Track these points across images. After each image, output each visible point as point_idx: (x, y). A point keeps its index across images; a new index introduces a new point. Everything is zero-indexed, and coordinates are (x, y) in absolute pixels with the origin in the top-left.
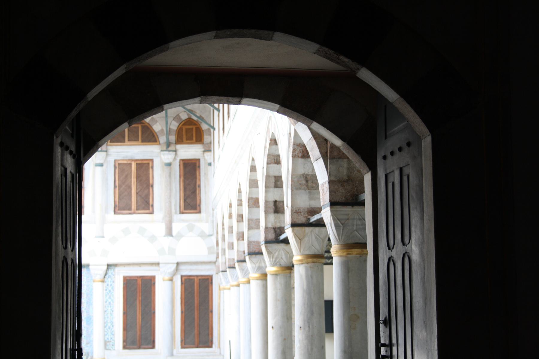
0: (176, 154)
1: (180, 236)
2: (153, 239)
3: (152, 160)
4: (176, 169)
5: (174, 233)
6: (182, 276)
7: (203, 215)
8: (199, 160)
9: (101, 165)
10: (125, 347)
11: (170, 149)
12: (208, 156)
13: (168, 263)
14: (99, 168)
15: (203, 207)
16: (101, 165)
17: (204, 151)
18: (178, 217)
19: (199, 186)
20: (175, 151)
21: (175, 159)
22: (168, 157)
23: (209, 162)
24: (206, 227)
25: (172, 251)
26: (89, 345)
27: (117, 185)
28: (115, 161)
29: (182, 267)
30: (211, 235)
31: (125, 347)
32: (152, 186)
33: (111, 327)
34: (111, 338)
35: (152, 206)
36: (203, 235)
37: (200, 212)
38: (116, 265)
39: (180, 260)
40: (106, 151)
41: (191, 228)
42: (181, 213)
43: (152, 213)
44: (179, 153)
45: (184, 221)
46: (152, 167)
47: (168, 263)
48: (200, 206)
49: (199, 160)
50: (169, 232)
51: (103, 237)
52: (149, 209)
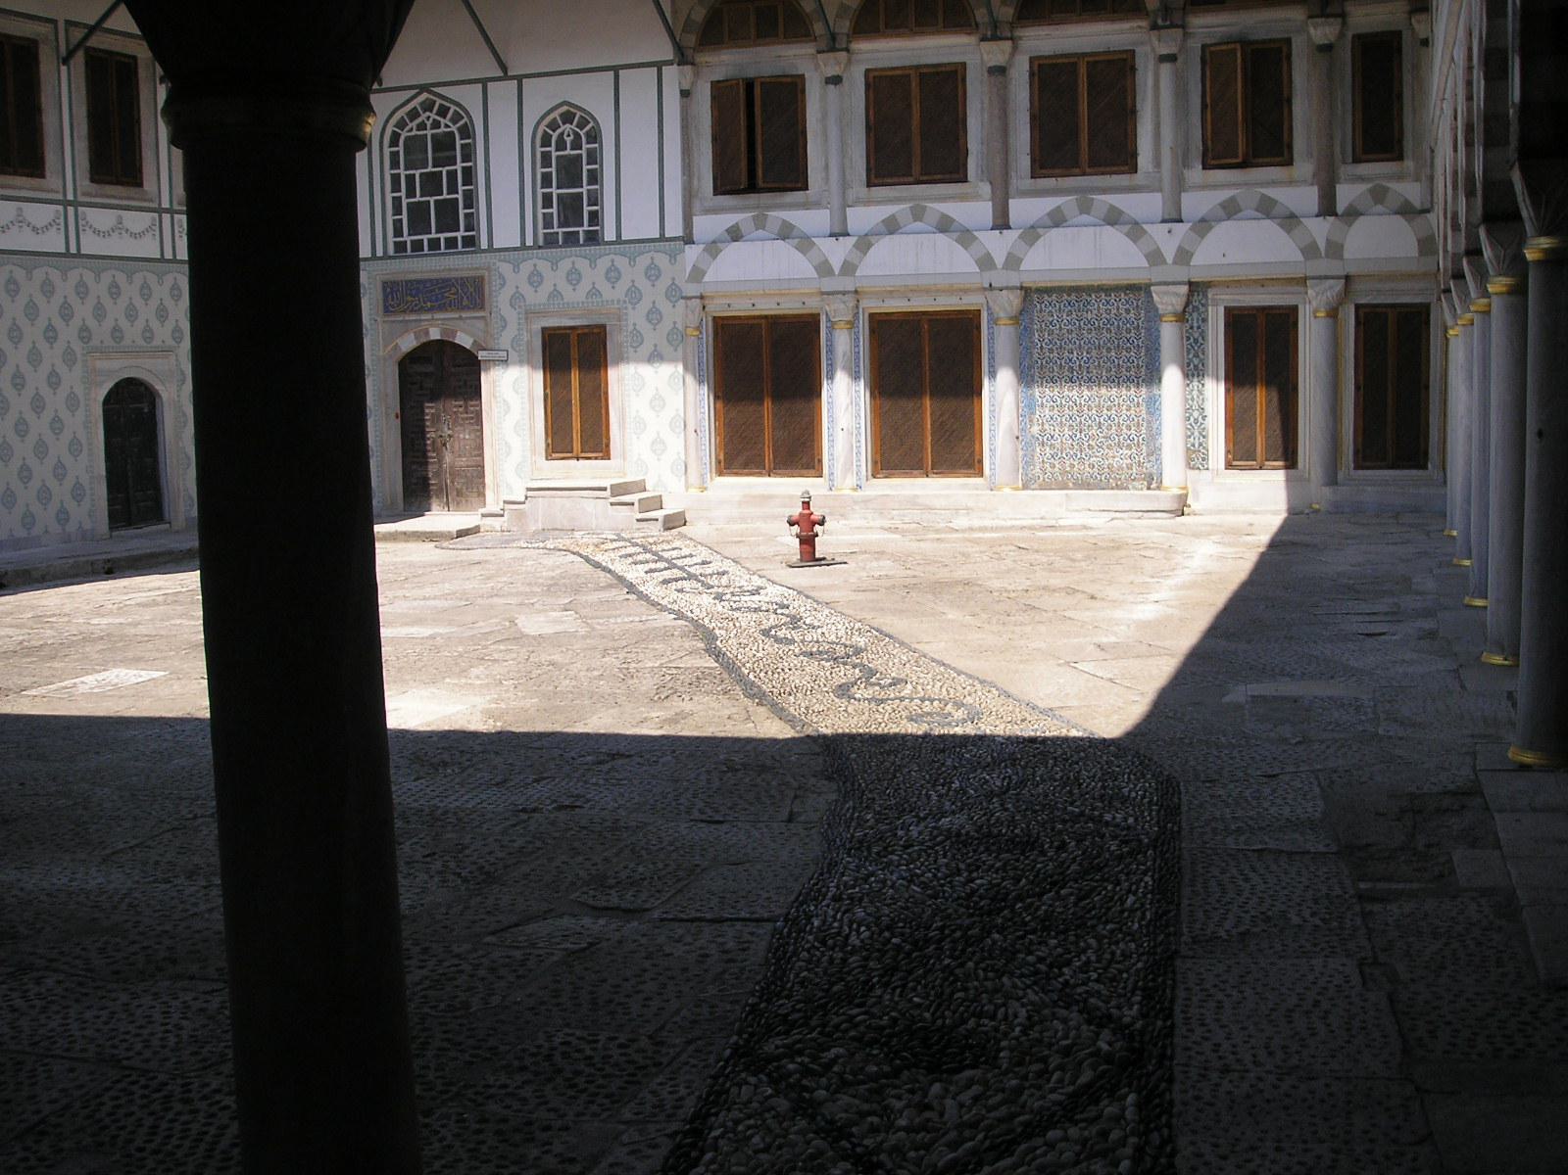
0: (1344, 24)
1: (1353, 214)
2: (1290, 221)
3: (1288, 41)
4: (1346, 55)
5: (1340, 208)
6: (1358, 307)
7: (1409, 164)
8: (1399, 33)
9: (1171, 58)
10: (1229, 466)
11: (1329, 11)
12: (1420, 28)
13: (1327, 278)
14: (1166, 69)
15: (1408, 144)
16: (1171, 58)
17: (1412, 12)
18: (1347, 170)
19: (1400, 96)
20: (1343, 15)
21: (1342, 35)
22: (1323, 32)
23: (1422, 36)
24: (1411, 191)
25: (1335, 250)
26: (1153, 458)
27: (1208, 101)
28: (1204, 47)
29: (1357, 286)
30: (1428, 211)
31: (1229, 466)
32: (1289, 101)
33: (1200, 419)
34: (1200, 444)
35: (1290, 147)
36: (1406, 211)
37: (1400, 157)
38: (1208, 285)
39: (1352, 270)
40: (1183, 27)
41: (1379, 195)
42: (1356, 160)
43: (1289, 163)
44: (1351, 20)
45: (1361, 179)
46: (1289, 56)
47: (1327, 278)
48: (1400, 141)
49: (1399, 33)
50: (1327, 208)
51: (1181, 221)
52: (1282, 155)
